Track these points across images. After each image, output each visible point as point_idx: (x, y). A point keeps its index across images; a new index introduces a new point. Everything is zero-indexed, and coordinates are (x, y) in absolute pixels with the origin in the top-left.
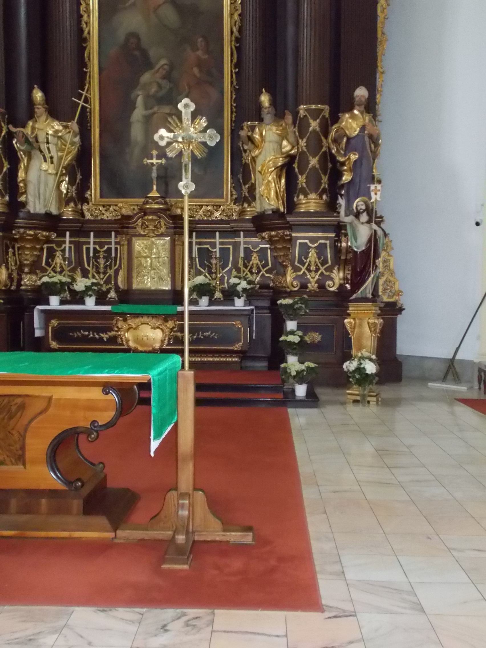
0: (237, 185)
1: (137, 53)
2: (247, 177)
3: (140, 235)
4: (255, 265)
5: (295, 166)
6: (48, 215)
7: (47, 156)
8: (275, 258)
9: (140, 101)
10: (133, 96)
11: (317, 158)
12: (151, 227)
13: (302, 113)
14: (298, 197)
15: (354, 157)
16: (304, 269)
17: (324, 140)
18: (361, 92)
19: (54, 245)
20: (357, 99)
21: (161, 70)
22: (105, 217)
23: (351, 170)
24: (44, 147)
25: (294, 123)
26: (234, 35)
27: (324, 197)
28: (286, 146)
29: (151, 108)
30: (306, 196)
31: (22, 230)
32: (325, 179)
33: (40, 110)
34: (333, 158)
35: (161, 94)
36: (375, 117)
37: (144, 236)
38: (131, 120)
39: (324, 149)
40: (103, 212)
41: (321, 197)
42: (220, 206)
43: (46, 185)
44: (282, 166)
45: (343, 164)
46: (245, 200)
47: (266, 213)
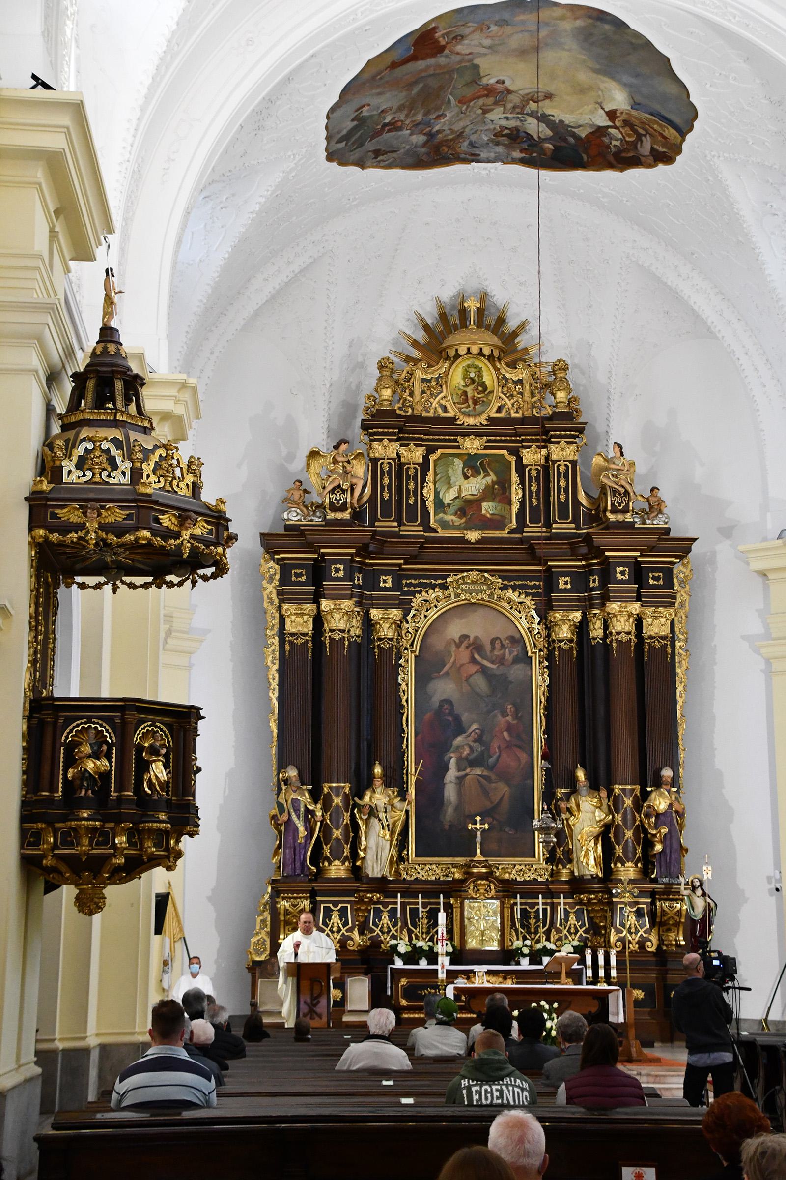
1: (450, 719)
3: (472, 898)
4: (572, 926)
5: (611, 835)
6: (384, 878)
7: (385, 823)
8: (591, 919)
9: (453, 762)
10: (446, 758)
11: (632, 831)
12: (482, 891)
14: (615, 864)
15: (664, 830)
17: (637, 815)
18: (667, 773)
19: (380, 906)
20: (664, 779)
21: (473, 733)
22: (420, 876)
23: (661, 842)
24: (382, 815)
25: (609, 797)
26: (542, 704)
27: (639, 865)
28: (600, 815)
29: (464, 770)
30: (623, 865)
31: (361, 894)
32: (639, 850)
33: (378, 782)
34: (645, 831)
35: (471, 757)
37: (476, 899)
38: (445, 781)
39: (637, 823)
40: (419, 870)
42: (532, 866)
45: (654, 836)
46: (560, 861)
47: (585, 877)
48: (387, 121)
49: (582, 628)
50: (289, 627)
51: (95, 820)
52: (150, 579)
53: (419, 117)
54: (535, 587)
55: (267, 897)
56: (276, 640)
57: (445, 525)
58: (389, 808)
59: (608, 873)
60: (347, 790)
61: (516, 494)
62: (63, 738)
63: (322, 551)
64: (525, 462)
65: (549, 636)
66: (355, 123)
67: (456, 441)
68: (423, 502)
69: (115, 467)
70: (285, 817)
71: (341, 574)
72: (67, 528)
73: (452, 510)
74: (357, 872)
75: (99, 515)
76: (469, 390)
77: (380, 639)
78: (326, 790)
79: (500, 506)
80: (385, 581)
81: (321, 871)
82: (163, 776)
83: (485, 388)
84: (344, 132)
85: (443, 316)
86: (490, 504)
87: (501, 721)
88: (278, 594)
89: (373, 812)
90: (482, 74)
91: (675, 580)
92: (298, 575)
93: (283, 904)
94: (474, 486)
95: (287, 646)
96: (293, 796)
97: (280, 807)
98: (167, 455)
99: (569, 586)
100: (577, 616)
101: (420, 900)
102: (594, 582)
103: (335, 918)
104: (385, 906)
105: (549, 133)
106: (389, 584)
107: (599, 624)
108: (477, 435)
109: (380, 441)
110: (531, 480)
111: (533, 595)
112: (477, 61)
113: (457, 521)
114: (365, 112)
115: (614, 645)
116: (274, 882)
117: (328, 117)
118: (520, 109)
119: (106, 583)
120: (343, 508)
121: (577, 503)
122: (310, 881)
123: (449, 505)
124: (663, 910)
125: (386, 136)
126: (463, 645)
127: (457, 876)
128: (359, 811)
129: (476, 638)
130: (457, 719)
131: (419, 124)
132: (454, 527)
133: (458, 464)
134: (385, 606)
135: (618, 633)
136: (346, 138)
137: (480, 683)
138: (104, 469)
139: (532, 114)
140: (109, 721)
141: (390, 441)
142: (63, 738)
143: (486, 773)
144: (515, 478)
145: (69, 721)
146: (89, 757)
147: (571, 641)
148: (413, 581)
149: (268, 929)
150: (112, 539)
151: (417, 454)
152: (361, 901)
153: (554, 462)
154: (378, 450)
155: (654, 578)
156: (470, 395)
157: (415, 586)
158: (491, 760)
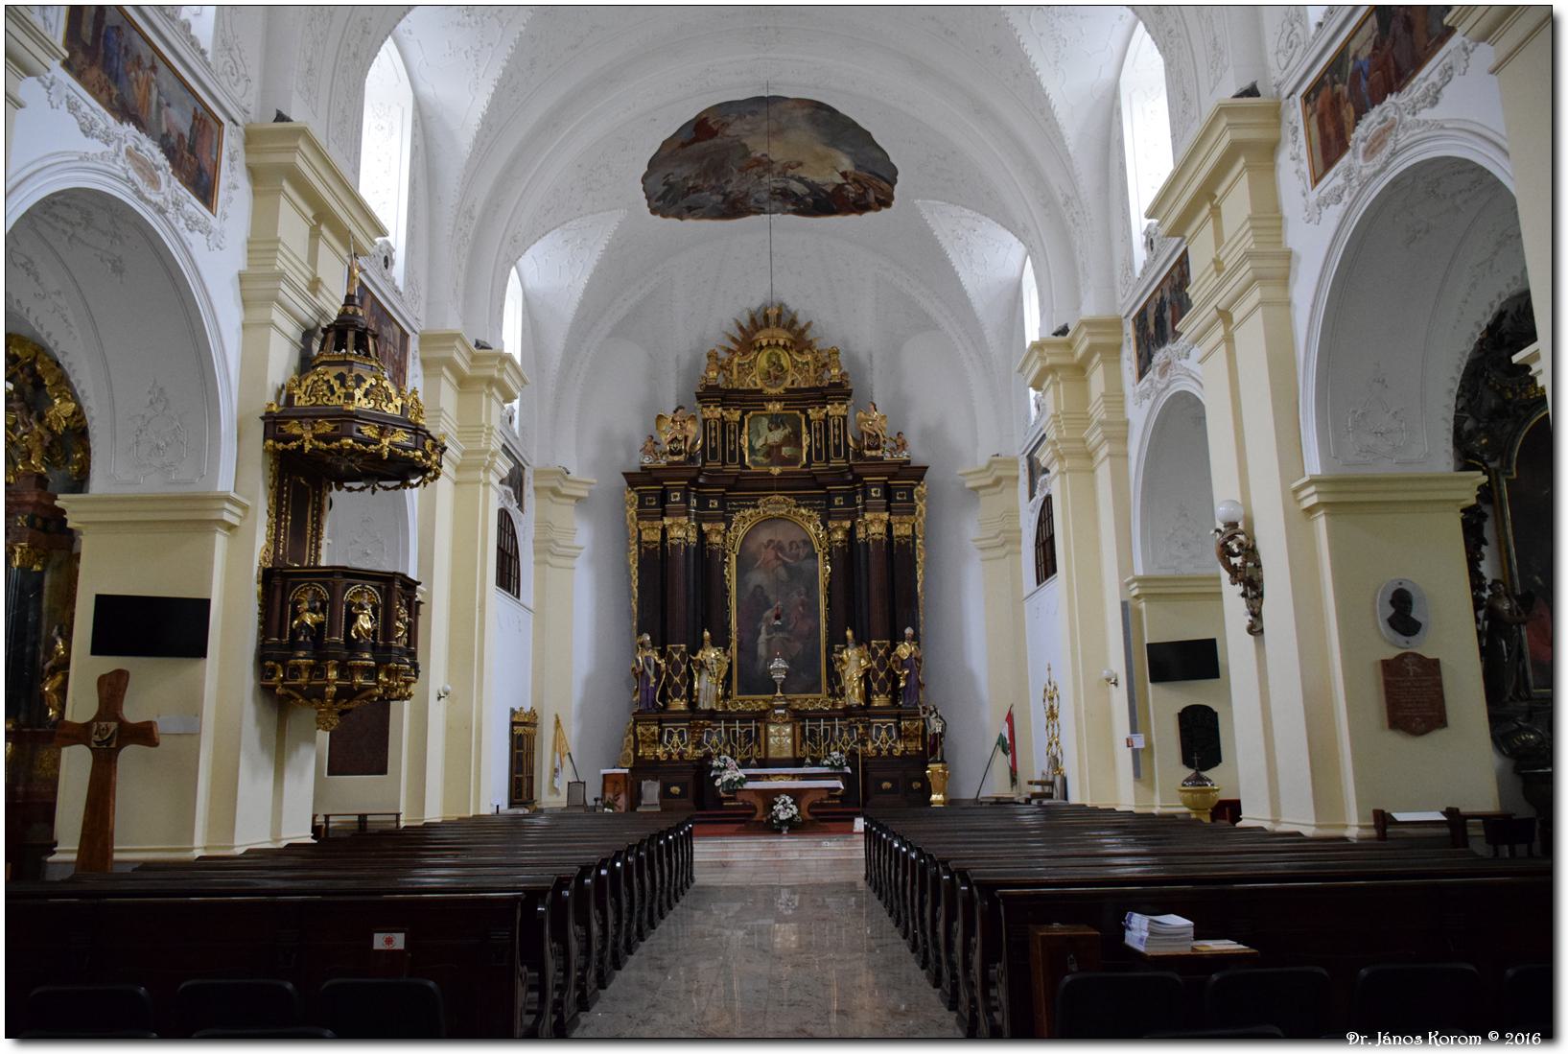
0: (831, 685)
2: (838, 680)
6: (712, 710)
9: (763, 628)
13: (873, 645)
15: (906, 672)
16: (879, 742)
18: (909, 631)
25: (868, 649)
30: (878, 696)
32: (889, 685)
33: (707, 643)
34: (894, 672)
36: (918, 645)
41: (887, 696)
43: (711, 690)
44: (861, 678)
45: (900, 675)
48: (690, 185)
49: (851, 533)
50: (644, 537)
51: (309, 659)
52: (398, 483)
53: (713, 182)
54: (819, 505)
55: (631, 724)
56: (636, 547)
57: (755, 463)
58: (715, 662)
59: (868, 701)
60: (683, 650)
61: (805, 441)
62: (291, 598)
63: (665, 483)
64: (811, 418)
65: (829, 539)
66: (666, 187)
67: (763, 405)
68: (741, 448)
69: (333, 392)
70: (638, 670)
71: (678, 499)
72: (288, 439)
73: (762, 453)
74: (692, 705)
75: (313, 428)
76: (771, 370)
77: (710, 544)
78: (669, 650)
79: (795, 450)
80: (713, 504)
81: (666, 705)
82: (368, 625)
83: (783, 368)
84: (660, 194)
85: (753, 320)
86: (788, 448)
87: (795, 598)
88: (637, 515)
89: (702, 665)
90: (750, 150)
91: (915, 497)
92: (649, 501)
93: (639, 729)
94: (776, 436)
95: (643, 550)
96: (646, 654)
97: (637, 661)
98: (377, 383)
99: (842, 503)
100: (847, 524)
101: (737, 725)
102: (859, 499)
103: (676, 738)
104: (715, 728)
105: (808, 191)
106: (678, 499)
107: (862, 529)
108: (777, 400)
109: (709, 407)
110: (815, 431)
111: (819, 510)
112: (744, 141)
113: (765, 461)
114: (672, 179)
115: (871, 542)
116: (634, 714)
117: (643, 182)
118: (783, 173)
119: (367, 487)
120: (679, 453)
121: (847, 446)
122: (658, 712)
123: (759, 450)
124: (906, 728)
125: (693, 196)
126: (771, 547)
127: (762, 707)
128: (694, 665)
129: (779, 542)
130: (766, 598)
131: (714, 187)
132: (762, 465)
133: (765, 421)
134: (712, 519)
135: (874, 534)
136: (663, 197)
137: (782, 572)
138: (324, 395)
139: (792, 177)
140: (324, 584)
141: (716, 406)
142: (291, 598)
143: (787, 636)
144: (804, 429)
145: (295, 585)
146: (307, 611)
147: (843, 541)
148: (734, 504)
149: (632, 746)
150: (323, 445)
151: (737, 415)
152: (696, 726)
153: (831, 417)
154: (708, 414)
155: (900, 496)
156: (772, 373)
157: (735, 506)
158: (791, 627)
